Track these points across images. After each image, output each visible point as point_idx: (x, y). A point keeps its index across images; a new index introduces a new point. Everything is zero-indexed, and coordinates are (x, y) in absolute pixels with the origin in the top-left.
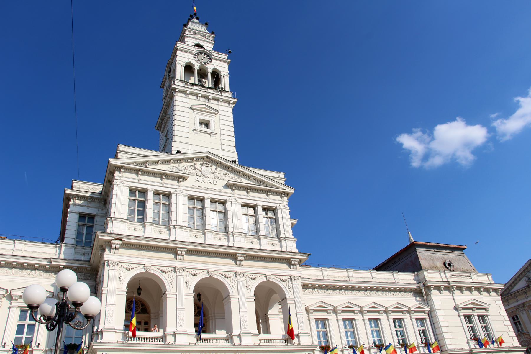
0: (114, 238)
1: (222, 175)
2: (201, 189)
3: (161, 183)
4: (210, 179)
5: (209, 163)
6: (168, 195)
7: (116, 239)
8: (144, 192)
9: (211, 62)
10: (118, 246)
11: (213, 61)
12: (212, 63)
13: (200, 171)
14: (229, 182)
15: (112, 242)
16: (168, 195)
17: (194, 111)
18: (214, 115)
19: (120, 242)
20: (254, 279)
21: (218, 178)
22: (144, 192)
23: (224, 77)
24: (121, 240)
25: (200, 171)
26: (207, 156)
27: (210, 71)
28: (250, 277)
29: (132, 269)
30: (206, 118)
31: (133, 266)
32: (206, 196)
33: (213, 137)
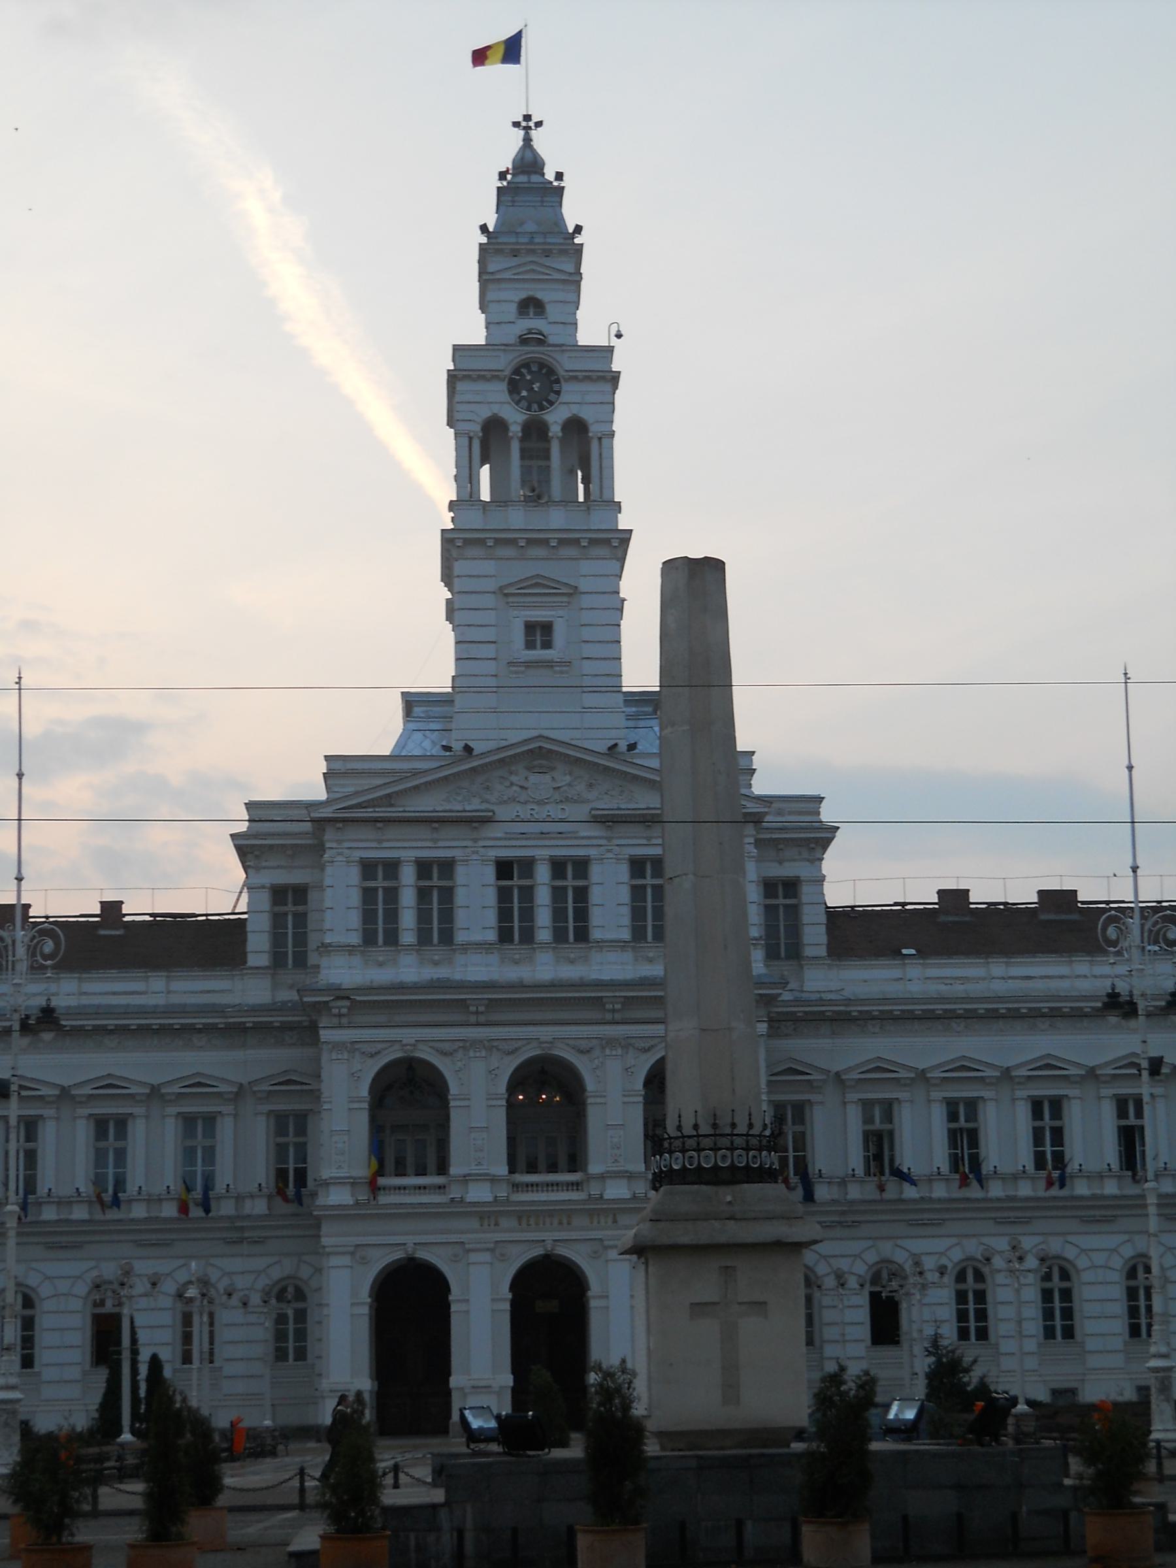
0: (332, 998)
1: (580, 787)
2: (527, 839)
3: (432, 840)
4: (548, 807)
5: (544, 762)
6: (447, 867)
7: (338, 998)
8: (392, 868)
9: (558, 393)
10: (344, 1011)
11: (566, 387)
12: (564, 397)
13: (522, 787)
14: (593, 812)
15: (332, 1004)
16: (447, 867)
17: (511, 599)
18: (565, 599)
19: (347, 1003)
20: (646, 1050)
21: (567, 800)
22: (392, 868)
23: (600, 439)
24: (348, 998)
25: (522, 787)
26: (540, 747)
27: (555, 430)
28: (637, 1045)
29: (376, 1053)
30: (539, 615)
31: (380, 1046)
32: (539, 853)
33: (561, 672)
